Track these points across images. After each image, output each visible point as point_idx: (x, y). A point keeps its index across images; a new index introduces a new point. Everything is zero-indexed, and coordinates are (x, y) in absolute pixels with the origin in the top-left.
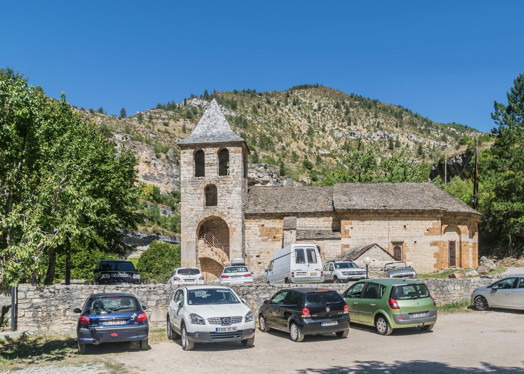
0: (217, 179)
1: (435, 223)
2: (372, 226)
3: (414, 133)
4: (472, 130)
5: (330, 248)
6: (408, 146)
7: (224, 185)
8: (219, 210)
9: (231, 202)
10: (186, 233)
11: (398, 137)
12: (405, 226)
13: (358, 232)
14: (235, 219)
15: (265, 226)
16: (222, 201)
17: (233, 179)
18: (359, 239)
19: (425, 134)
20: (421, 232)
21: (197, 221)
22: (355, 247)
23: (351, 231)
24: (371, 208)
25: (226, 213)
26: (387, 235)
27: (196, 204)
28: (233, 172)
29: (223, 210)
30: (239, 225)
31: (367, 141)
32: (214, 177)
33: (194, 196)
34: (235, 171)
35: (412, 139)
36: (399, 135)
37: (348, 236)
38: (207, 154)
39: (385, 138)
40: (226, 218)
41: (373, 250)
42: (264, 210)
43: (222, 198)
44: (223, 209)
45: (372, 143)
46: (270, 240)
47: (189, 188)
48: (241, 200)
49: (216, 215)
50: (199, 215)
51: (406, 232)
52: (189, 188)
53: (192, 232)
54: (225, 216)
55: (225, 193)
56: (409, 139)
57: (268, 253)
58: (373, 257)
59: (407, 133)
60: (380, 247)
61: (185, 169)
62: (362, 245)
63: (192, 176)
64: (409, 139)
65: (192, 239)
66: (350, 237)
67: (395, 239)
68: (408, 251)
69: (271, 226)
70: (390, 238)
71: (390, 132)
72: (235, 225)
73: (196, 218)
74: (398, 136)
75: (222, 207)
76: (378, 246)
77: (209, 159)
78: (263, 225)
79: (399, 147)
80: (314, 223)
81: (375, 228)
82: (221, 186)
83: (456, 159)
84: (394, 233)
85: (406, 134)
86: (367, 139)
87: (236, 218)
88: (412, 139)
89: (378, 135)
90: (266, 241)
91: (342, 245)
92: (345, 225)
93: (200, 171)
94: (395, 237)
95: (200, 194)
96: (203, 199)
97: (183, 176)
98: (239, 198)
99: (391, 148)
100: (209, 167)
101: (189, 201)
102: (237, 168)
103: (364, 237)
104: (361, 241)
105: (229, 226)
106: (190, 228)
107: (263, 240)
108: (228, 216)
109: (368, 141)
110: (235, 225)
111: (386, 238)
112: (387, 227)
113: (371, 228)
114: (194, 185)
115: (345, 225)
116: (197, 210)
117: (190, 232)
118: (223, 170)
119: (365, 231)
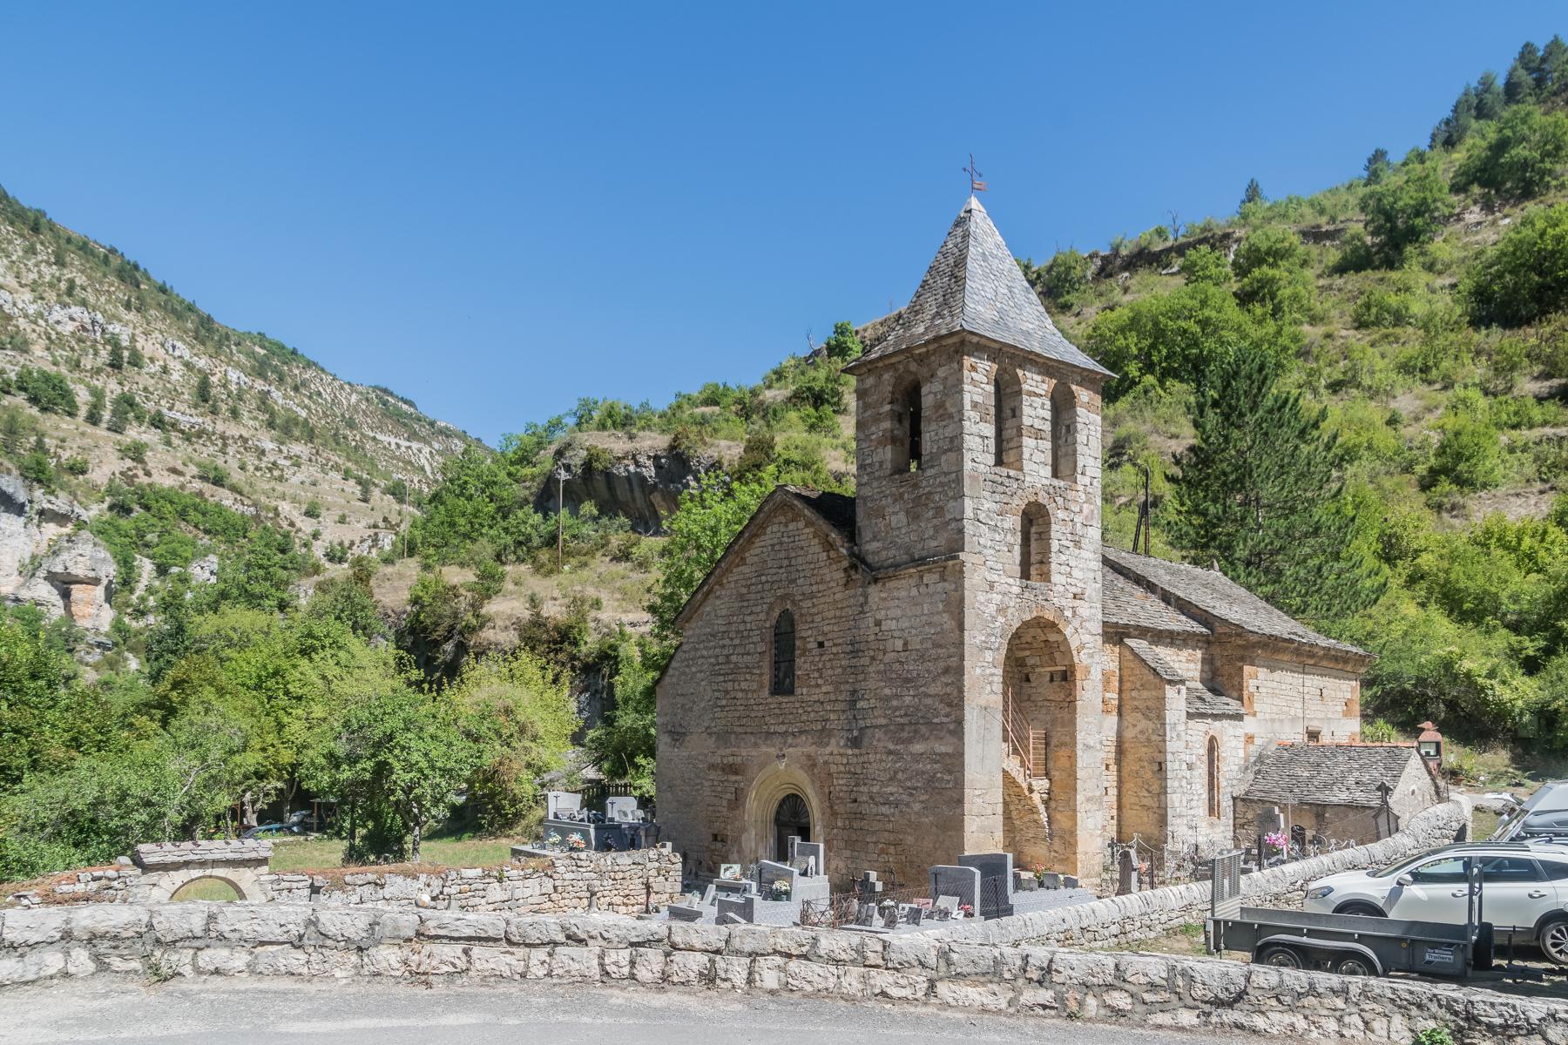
3: (181, 339)
4: (309, 364)
6: (165, 370)
10: (978, 671)
11: (133, 339)
19: (211, 350)
20: (1339, 709)
25: (1068, 613)
27: (1000, 566)
29: (1064, 602)
31: (34, 326)
33: (998, 538)
35: (177, 353)
36: (137, 332)
39: (95, 331)
43: (1063, 558)
45: (54, 336)
47: (987, 505)
50: (1010, 611)
52: (986, 506)
53: (993, 670)
54: (1066, 620)
56: (167, 351)
59: (161, 332)
64: (167, 351)
65: (993, 697)
66: (1254, 715)
71: (113, 318)
74: (134, 335)
79: (141, 368)
83: (637, 464)
85: (157, 334)
86: (35, 323)
88: (177, 353)
89: (72, 319)
92: (1257, 678)
93: (1005, 450)
99: (116, 365)
102: (1091, 461)
103: (1274, 716)
105: (1076, 660)
106: (989, 656)
109: (37, 329)
114: (997, 497)
115: (1257, 678)
116: (1004, 588)
117: (988, 672)
118: (1063, 461)
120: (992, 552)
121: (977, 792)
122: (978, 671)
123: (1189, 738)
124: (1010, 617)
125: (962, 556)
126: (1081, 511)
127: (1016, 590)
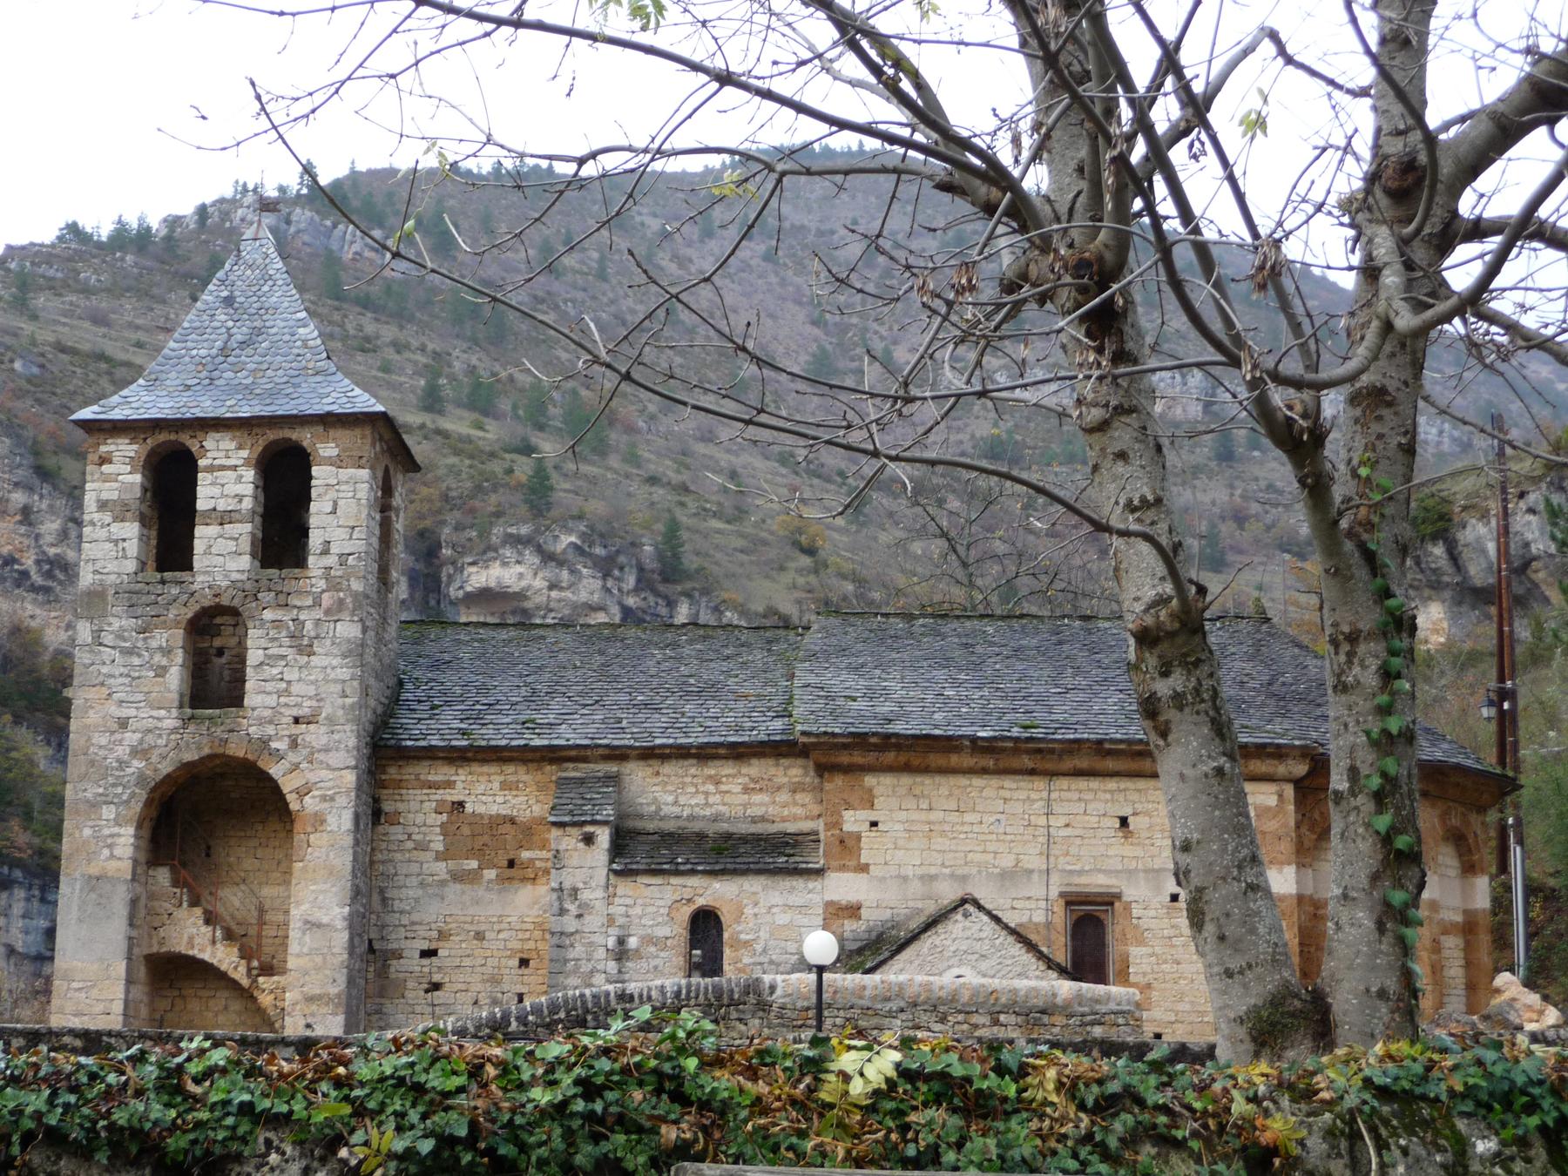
0: (248, 586)
1: (1268, 809)
2: (969, 817)
5: (768, 918)
7: (279, 614)
8: (252, 730)
9: (311, 691)
12: (1124, 822)
13: (901, 843)
14: (324, 774)
15: (469, 808)
16: (269, 687)
17: (322, 584)
18: (905, 879)
21: (141, 779)
22: (887, 914)
23: (868, 838)
24: (967, 731)
26: (1036, 863)
27: (140, 697)
28: (325, 552)
29: (270, 730)
30: (342, 801)
32: (235, 576)
33: (136, 661)
34: (334, 549)
37: (853, 863)
38: (211, 469)
40: (284, 765)
41: (957, 927)
42: (464, 733)
44: (271, 722)
46: (490, 874)
48: (356, 683)
49: (237, 749)
50: (156, 752)
51: (1128, 851)
52: (116, 624)
53: (116, 830)
54: (278, 756)
55: (283, 651)
57: (480, 936)
58: (954, 961)
60: (989, 913)
61: (102, 533)
62: (920, 905)
63: (131, 566)
65: (114, 864)
66: (864, 868)
67: (1076, 880)
68: (1141, 942)
69: (494, 810)
70: (1055, 879)
72: (324, 798)
73: (137, 764)
75: (268, 713)
76: (980, 907)
77: (216, 491)
78: (461, 804)
80: (700, 799)
81: (984, 828)
82: (268, 615)
84: (1073, 850)
87: (329, 768)
90: (472, 882)
91: (829, 904)
94: (1080, 873)
95: (167, 652)
96: (175, 678)
97: (90, 567)
98: (344, 673)
100: (213, 530)
101: (112, 681)
103: (933, 870)
104: (916, 887)
105: (294, 806)
106: (108, 812)
107: (458, 877)
108: (292, 757)
110: (324, 798)
111: (1035, 877)
112: (1042, 821)
113: (966, 828)
114: (139, 611)
117: (106, 832)
119: (939, 843)
120: (127, 680)
121: (75, 985)
122: (87, 832)
123: (616, 910)
124: (154, 759)
125: (69, 693)
126: (317, 603)
127: (170, 723)
